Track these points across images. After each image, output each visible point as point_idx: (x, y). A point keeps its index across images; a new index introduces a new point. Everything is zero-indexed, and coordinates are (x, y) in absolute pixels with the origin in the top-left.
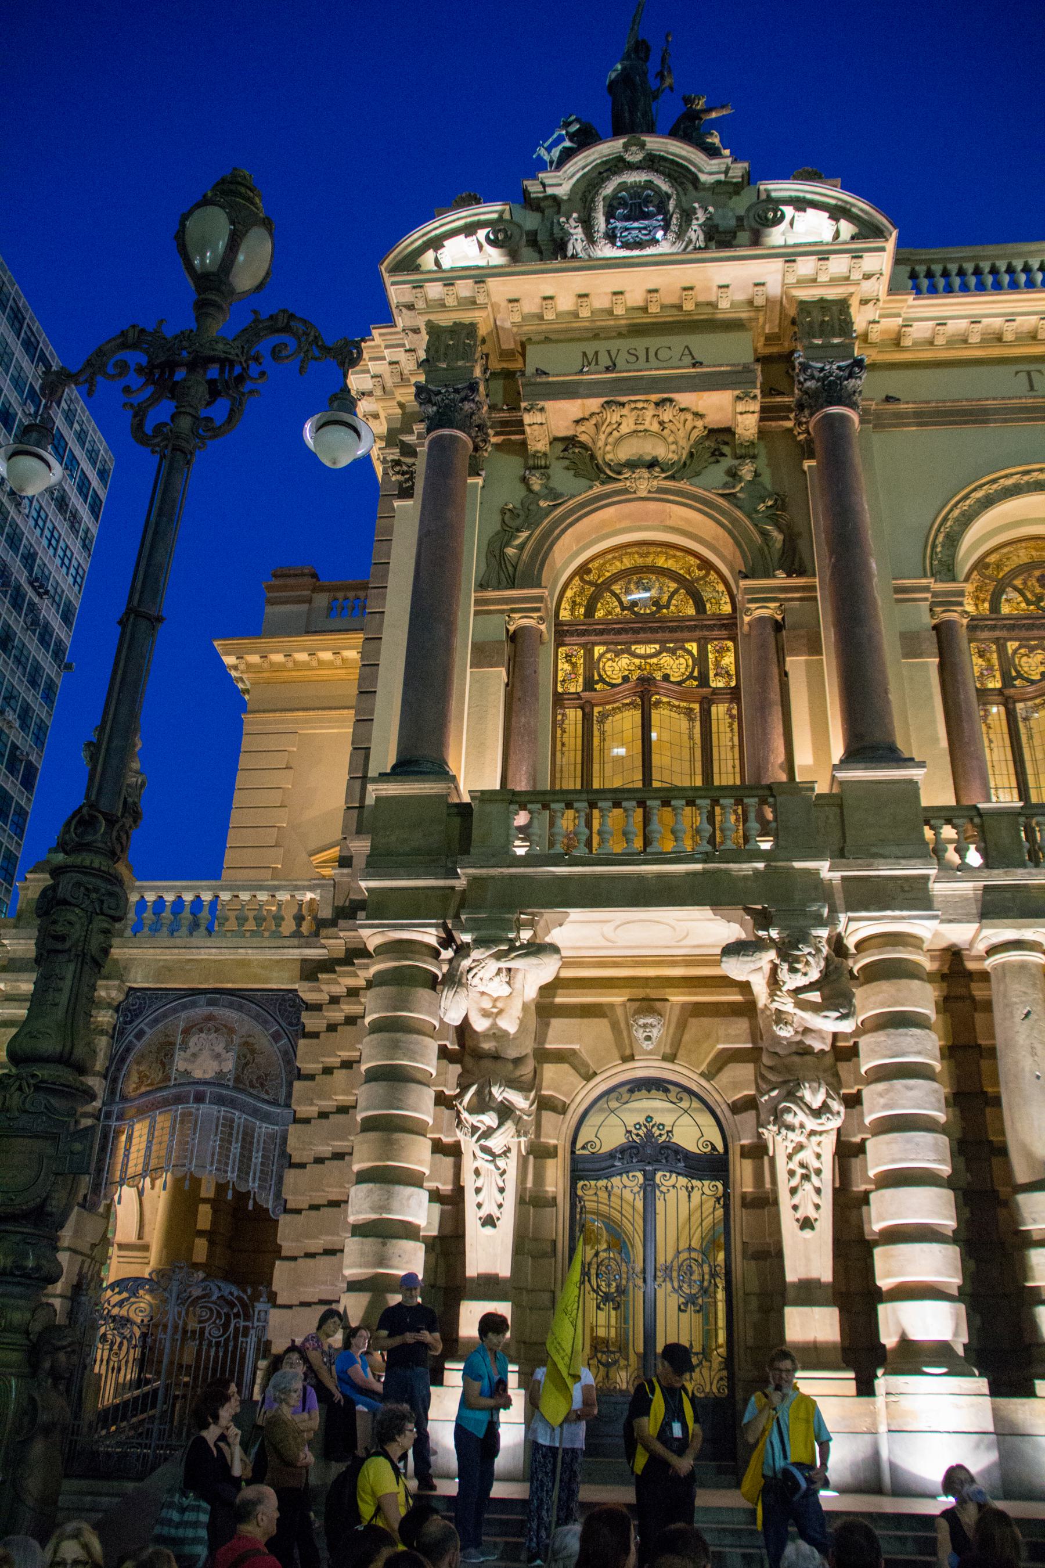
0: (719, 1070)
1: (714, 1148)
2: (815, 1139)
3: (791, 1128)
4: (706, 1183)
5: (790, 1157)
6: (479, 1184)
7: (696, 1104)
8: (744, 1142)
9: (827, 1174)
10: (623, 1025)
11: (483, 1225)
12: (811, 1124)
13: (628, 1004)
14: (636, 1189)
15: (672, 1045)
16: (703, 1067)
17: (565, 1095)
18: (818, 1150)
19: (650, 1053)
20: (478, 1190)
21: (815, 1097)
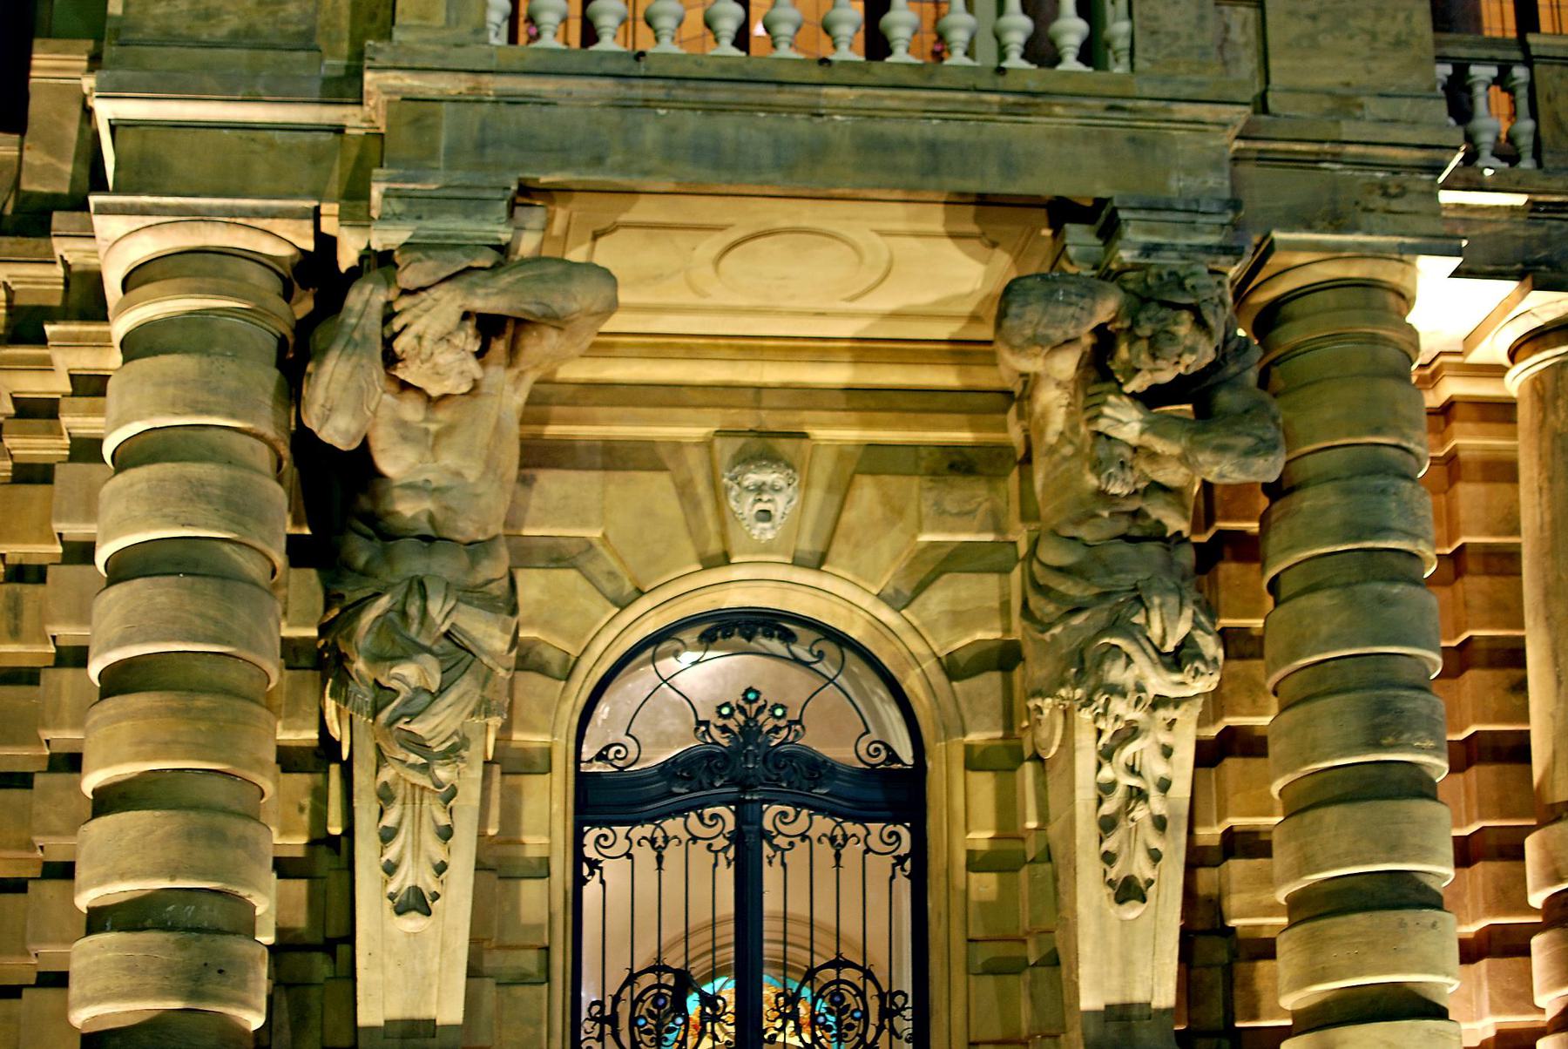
0: (921, 587)
1: (893, 757)
2: (1161, 713)
3: (1117, 691)
4: (875, 827)
5: (1107, 755)
6: (390, 819)
7: (855, 665)
8: (974, 737)
9: (1181, 790)
10: (702, 488)
11: (400, 910)
12: (1159, 683)
13: (718, 443)
14: (721, 842)
15: (814, 535)
16: (885, 581)
17: (573, 637)
18: (1165, 738)
19: (768, 548)
20: (388, 836)
21: (1170, 623)
